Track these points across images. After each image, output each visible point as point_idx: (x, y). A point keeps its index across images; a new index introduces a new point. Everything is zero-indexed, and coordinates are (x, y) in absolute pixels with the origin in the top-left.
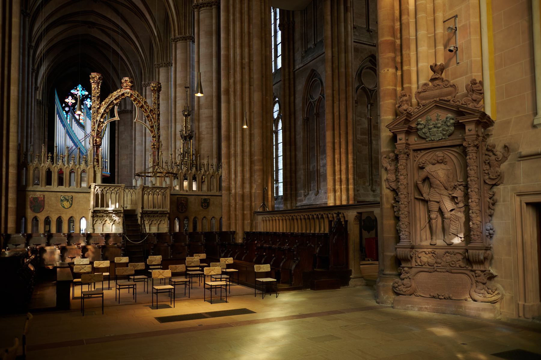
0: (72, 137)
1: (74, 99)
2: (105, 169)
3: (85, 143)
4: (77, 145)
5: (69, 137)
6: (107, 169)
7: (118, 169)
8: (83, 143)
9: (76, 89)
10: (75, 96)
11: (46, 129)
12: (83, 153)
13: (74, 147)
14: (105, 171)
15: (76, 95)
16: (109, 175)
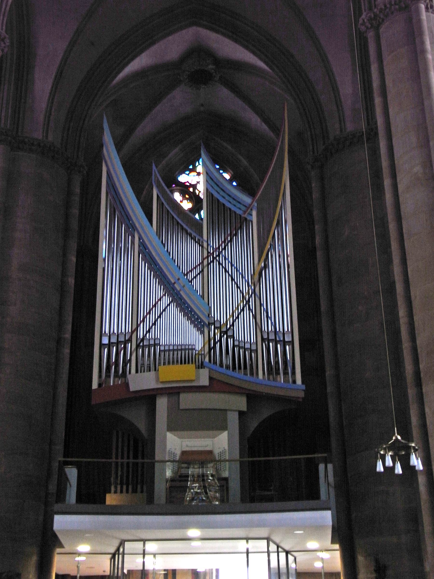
0: (156, 264)
1: (187, 199)
2: (286, 373)
3: (206, 285)
4: (174, 289)
5: (150, 265)
6: (294, 373)
7: (337, 367)
8: (197, 284)
9: (194, 170)
10: (191, 190)
11: (73, 245)
12: (202, 321)
13: (166, 300)
14: (286, 381)
15: (194, 187)
16: (302, 395)
